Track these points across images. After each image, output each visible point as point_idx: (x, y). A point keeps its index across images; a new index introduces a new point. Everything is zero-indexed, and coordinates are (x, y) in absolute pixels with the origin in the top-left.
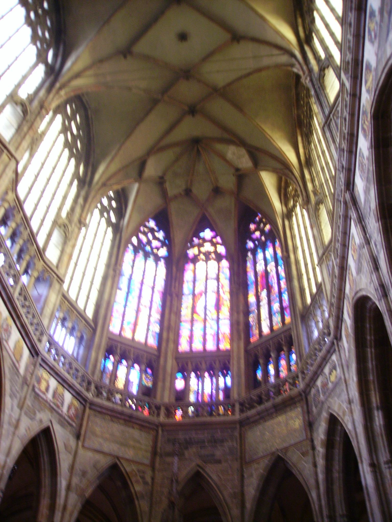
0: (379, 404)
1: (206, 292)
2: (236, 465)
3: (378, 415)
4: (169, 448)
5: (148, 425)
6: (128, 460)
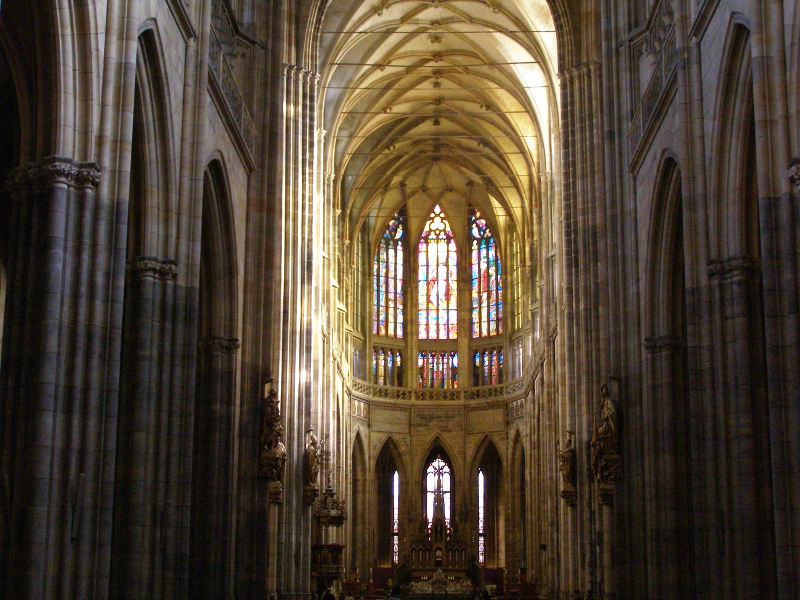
2: (461, 434)
4: (419, 421)
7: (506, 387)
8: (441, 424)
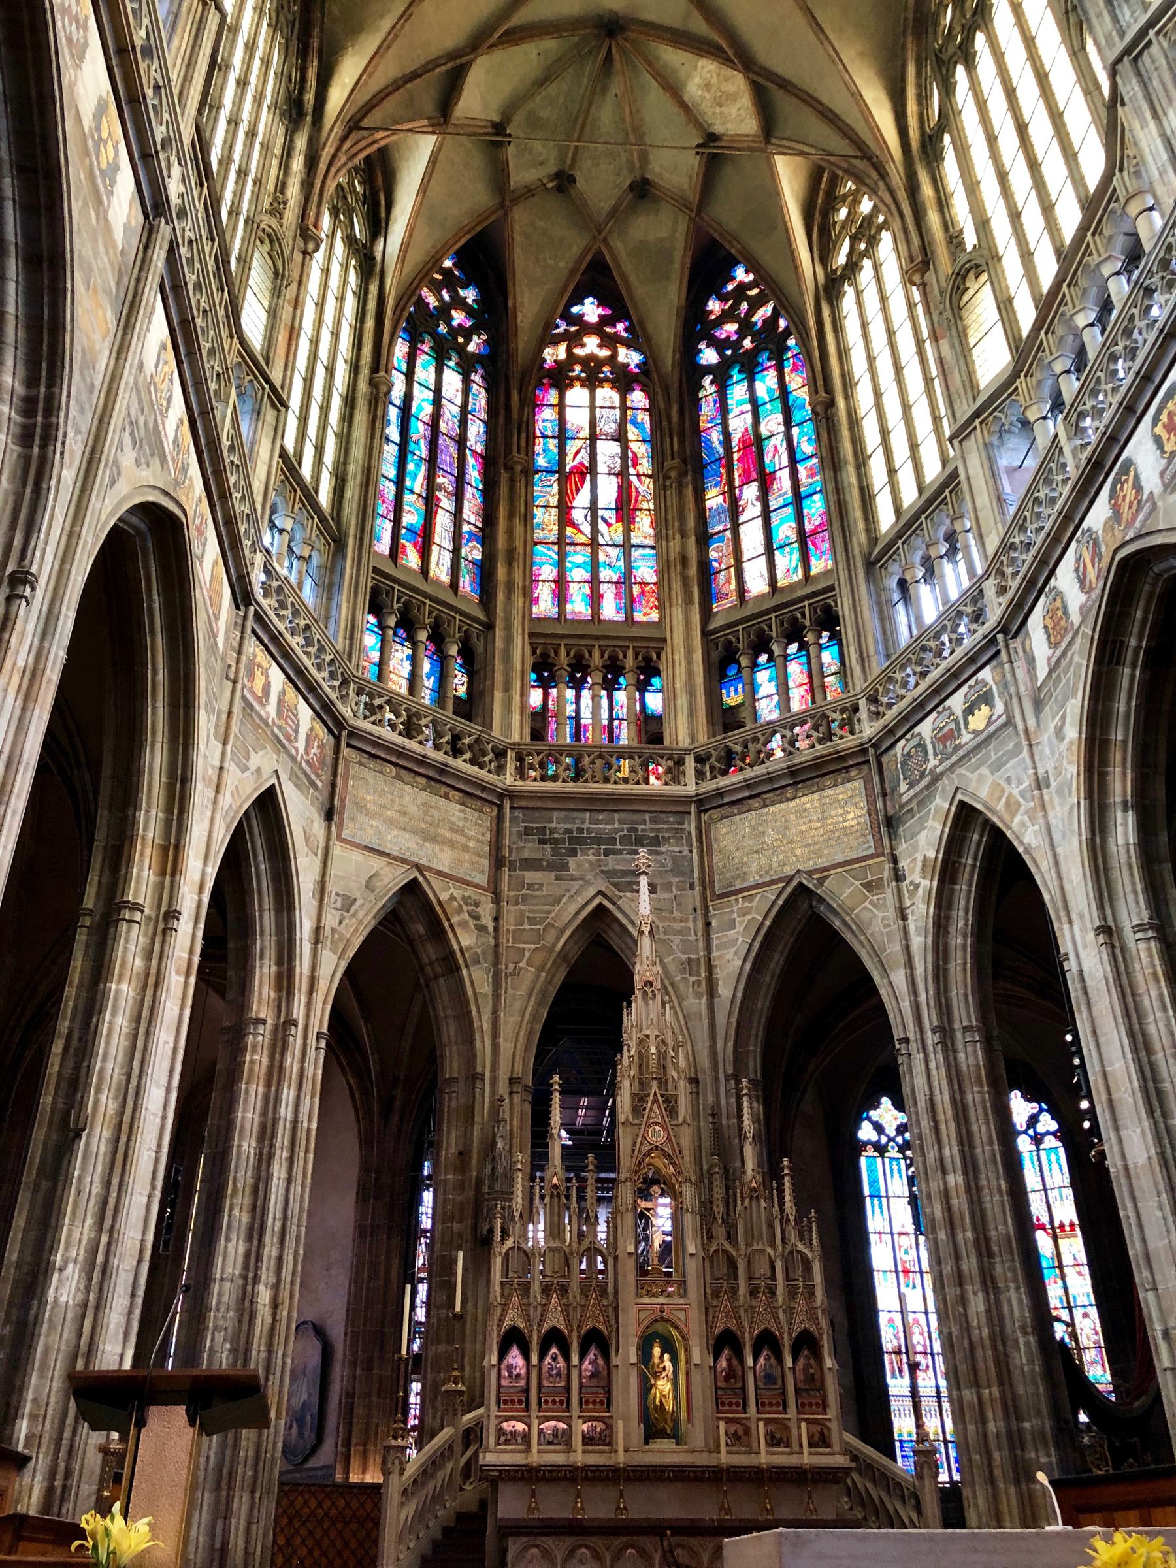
1: (592, 469)
3: (1125, 819)
5: (478, 793)
6: (439, 873)
7: (873, 700)
8: (612, 863)
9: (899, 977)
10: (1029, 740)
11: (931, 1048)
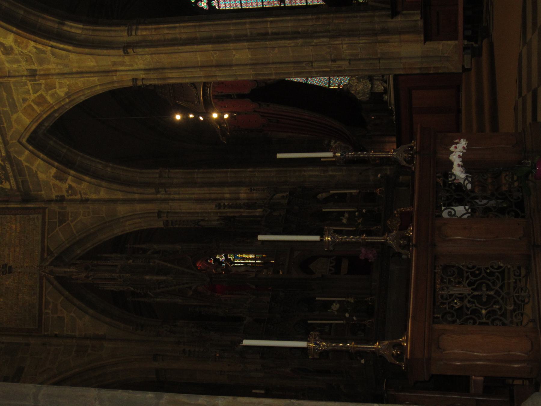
0: (58, 20)
3: (68, 26)
9: (122, 209)
10: (6, 77)
11: (167, 196)
